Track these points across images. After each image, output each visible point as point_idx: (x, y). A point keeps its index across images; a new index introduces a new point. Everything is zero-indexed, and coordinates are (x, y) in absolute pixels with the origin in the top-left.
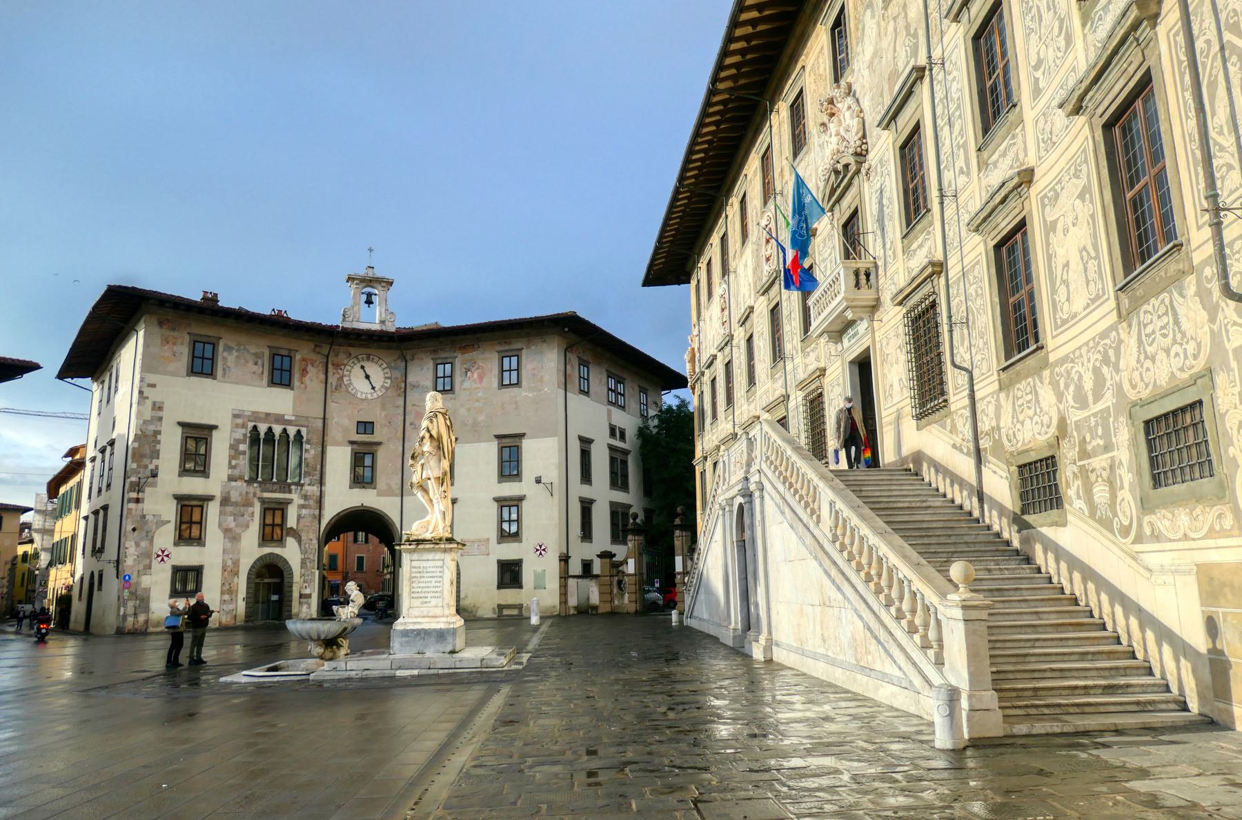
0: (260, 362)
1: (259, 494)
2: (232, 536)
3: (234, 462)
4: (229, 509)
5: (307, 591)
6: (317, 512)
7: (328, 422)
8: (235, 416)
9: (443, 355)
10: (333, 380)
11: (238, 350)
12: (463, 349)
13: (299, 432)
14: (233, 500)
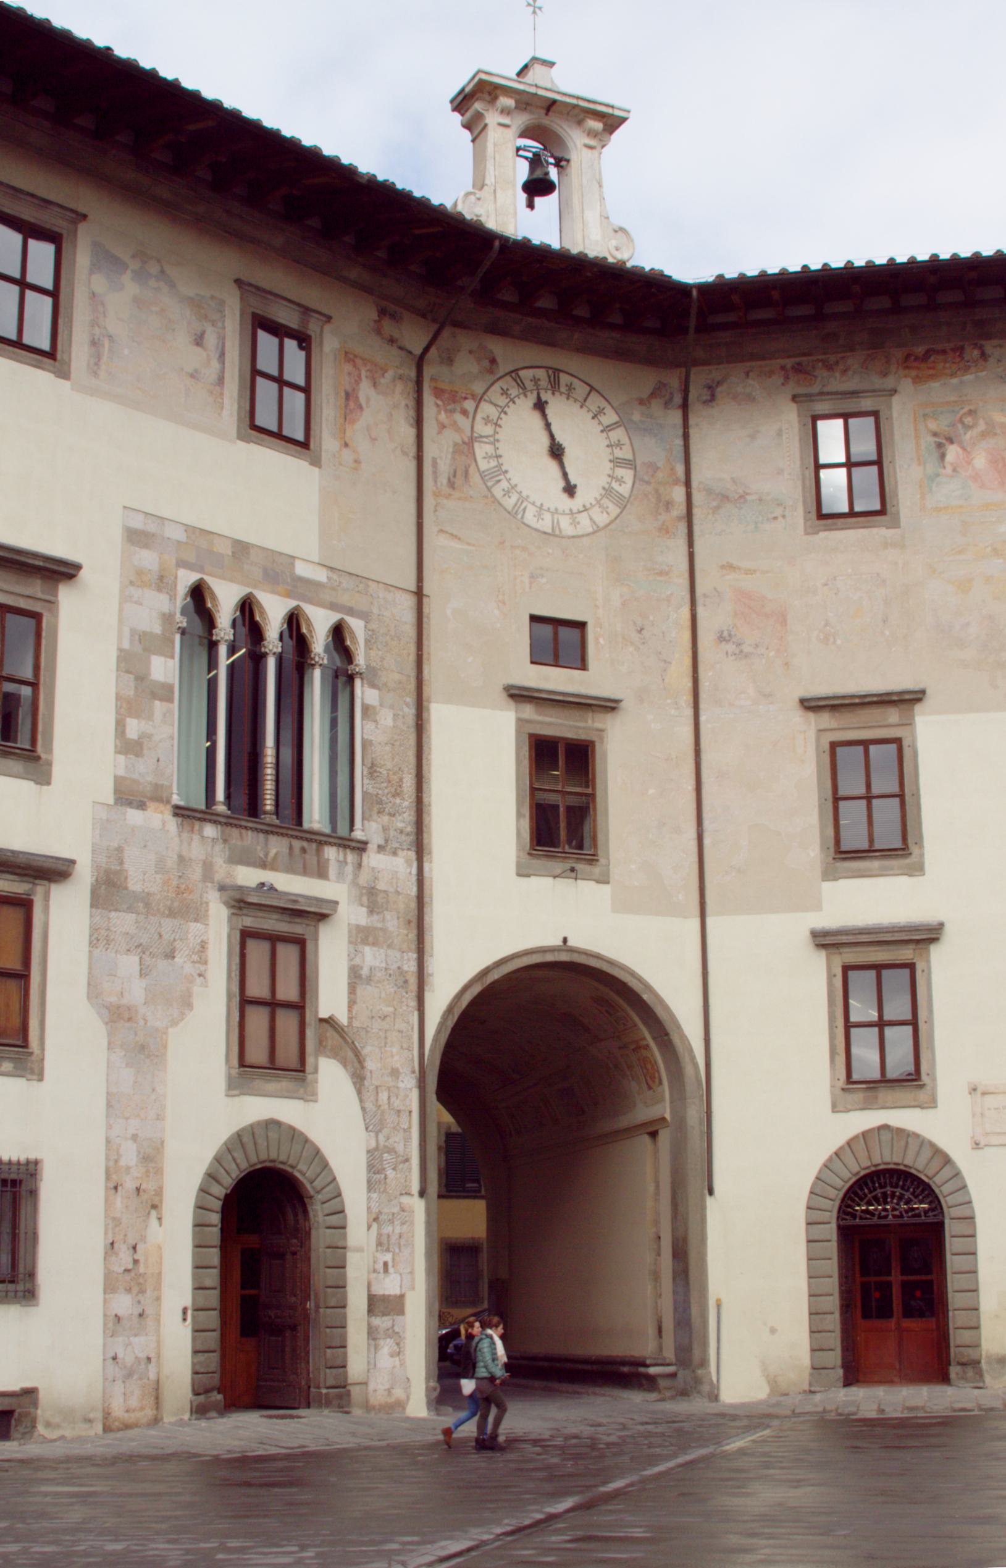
0: (211, 339)
1: (222, 870)
2: (137, 1043)
3: (134, 729)
4: (123, 922)
5: (389, 1286)
6: (411, 966)
7: (431, 608)
8: (136, 538)
9: (837, 383)
10: (439, 448)
11: (141, 276)
12: (920, 363)
13: (338, 632)
14: (135, 884)
